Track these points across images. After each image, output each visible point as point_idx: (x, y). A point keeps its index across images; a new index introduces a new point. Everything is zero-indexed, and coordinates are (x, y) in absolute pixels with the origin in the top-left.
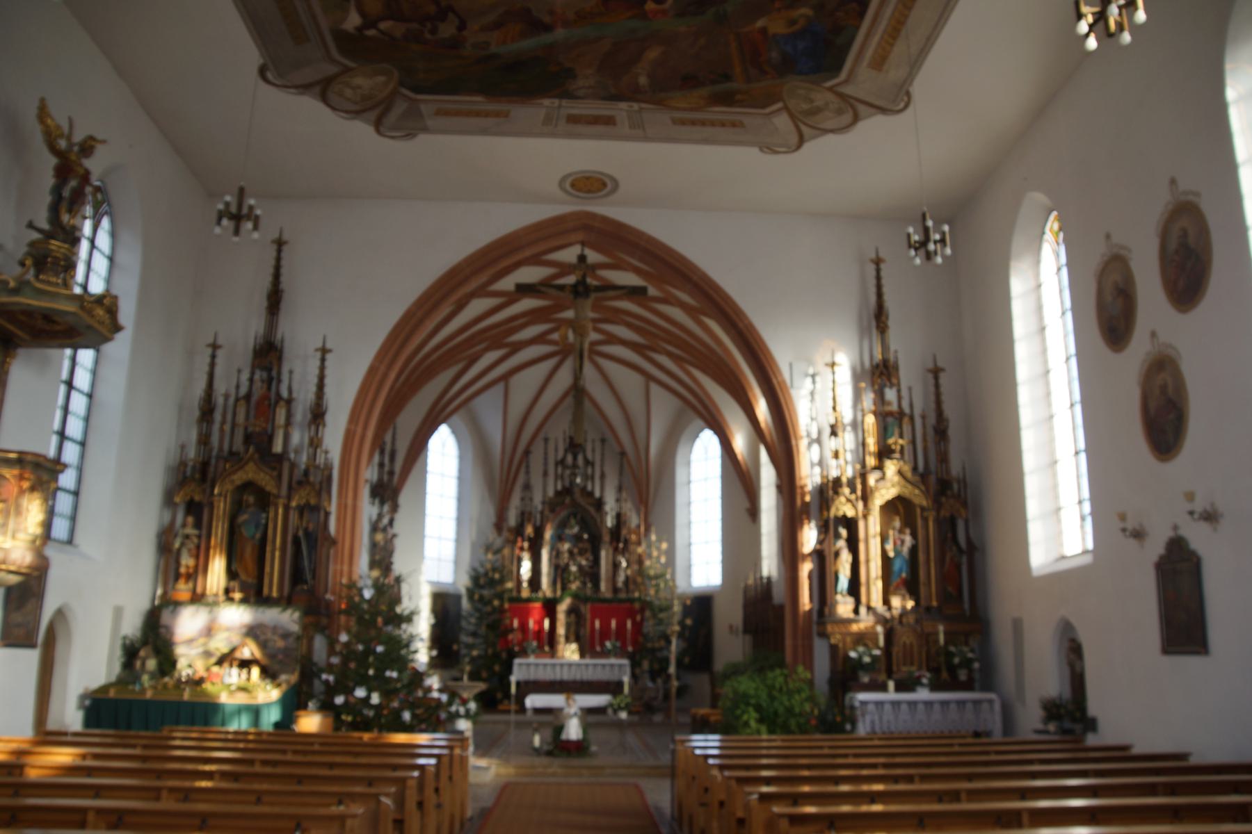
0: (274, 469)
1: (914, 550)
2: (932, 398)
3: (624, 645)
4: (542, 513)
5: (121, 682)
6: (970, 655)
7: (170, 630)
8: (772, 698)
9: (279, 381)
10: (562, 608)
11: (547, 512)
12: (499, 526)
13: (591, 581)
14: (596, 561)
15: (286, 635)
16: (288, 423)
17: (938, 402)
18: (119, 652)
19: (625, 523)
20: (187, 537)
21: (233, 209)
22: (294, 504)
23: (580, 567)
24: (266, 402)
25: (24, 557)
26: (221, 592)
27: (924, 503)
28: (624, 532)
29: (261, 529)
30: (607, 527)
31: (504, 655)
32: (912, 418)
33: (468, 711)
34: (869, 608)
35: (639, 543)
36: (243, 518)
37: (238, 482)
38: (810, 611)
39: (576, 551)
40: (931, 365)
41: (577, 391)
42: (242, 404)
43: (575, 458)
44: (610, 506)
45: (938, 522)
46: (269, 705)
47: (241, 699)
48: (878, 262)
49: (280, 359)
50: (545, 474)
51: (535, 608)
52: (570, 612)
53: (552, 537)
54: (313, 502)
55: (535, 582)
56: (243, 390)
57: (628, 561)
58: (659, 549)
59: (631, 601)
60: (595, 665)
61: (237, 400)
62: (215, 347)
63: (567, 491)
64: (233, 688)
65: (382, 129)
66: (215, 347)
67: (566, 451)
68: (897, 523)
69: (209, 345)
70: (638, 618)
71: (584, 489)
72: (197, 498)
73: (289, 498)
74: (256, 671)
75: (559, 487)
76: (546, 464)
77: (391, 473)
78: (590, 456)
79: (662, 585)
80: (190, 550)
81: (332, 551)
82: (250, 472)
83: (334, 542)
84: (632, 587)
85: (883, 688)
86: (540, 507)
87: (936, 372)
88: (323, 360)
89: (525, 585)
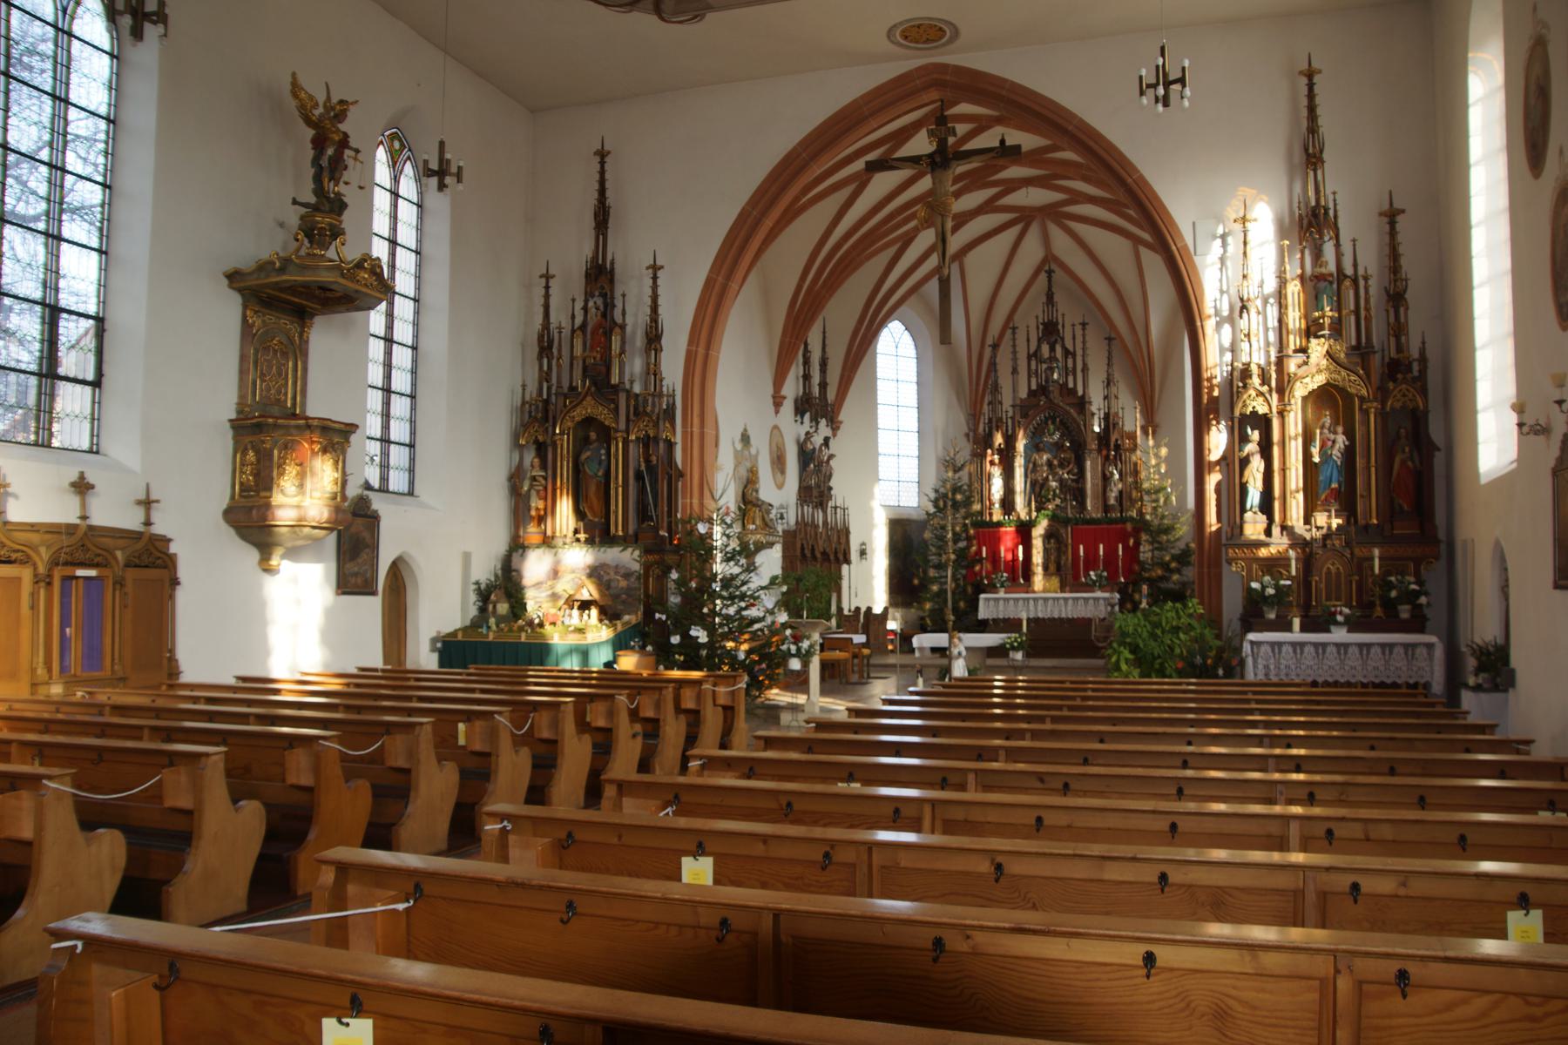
0: (613, 401)
1: (1349, 453)
2: (1387, 250)
4: (1013, 418)
5: (477, 624)
6: (1413, 587)
7: (519, 572)
8: (1153, 636)
9: (614, 306)
10: (1038, 532)
11: (1018, 418)
12: (969, 440)
15: (627, 576)
16: (623, 352)
17: (1394, 255)
18: (473, 597)
19: (1115, 425)
20: (534, 479)
21: (434, 166)
22: (633, 437)
23: (1061, 481)
24: (601, 331)
25: (322, 514)
26: (570, 534)
27: (1364, 392)
29: (605, 464)
31: (969, 589)
32: (1355, 281)
33: (799, 649)
34: (1284, 528)
36: (583, 457)
37: (578, 419)
38: (1219, 530)
39: (1056, 462)
40: (1386, 206)
41: (1049, 265)
42: (579, 332)
43: (1052, 349)
44: (1097, 404)
45: (1383, 415)
46: (599, 644)
47: (573, 640)
48: (1310, 75)
49: (612, 281)
50: (1015, 371)
51: (1006, 532)
52: (1048, 536)
53: (1026, 446)
54: (652, 434)
55: (1008, 504)
56: (579, 320)
57: (1121, 475)
58: (1157, 456)
59: (1123, 520)
60: (1074, 599)
61: (573, 331)
62: (547, 277)
63: (1043, 390)
64: (572, 628)
65: (664, 15)
66: (547, 277)
67: (1040, 341)
68: (1328, 421)
69: (541, 277)
70: (1131, 542)
71: (1063, 387)
72: (541, 438)
73: (627, 431)
74: (594, 612)
75: (1034, 387)
76: (1015, 359)
77: (823, 385)
78: (1069, 346)
79: (1162, 500)
80: (538, 492)
81: (680, 483)
82: (589, 408)
83: (681, 475)
84: (1126, 503)
85: (1288, 628)
86: (1010, 414)
87: (1391, 216)
88: (655, 278)
89: (997, 506)
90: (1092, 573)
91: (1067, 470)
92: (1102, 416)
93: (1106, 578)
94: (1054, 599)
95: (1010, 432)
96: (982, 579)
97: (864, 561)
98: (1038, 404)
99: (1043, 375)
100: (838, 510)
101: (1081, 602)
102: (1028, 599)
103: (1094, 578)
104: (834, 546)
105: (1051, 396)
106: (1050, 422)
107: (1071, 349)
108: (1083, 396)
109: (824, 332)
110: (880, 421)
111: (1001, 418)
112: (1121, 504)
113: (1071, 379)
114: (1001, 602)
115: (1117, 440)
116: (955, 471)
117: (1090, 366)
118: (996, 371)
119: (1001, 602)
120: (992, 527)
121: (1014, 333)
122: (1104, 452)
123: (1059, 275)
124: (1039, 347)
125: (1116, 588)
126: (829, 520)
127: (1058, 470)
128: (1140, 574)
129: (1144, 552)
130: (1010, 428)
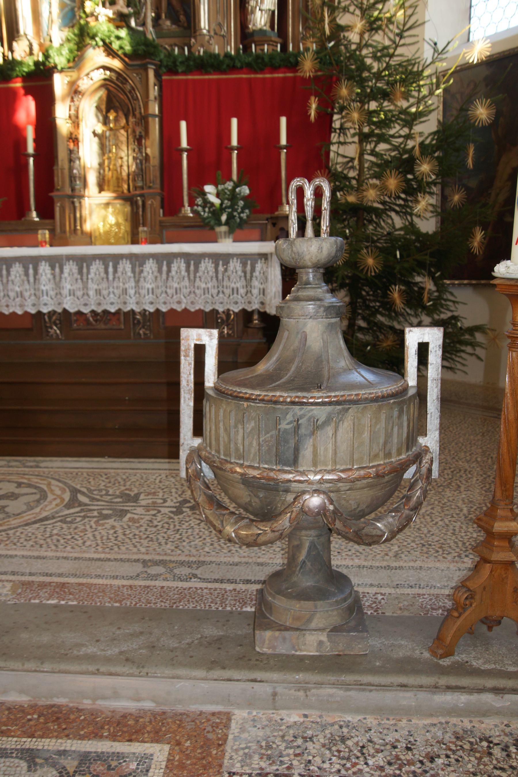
60: (158, 258)
90: (209, 189)
93: (244, 198)
94: (104, 258)
102: (36, 261)
103: (216, 201)
112: (282, 32)
129: (340, 143)
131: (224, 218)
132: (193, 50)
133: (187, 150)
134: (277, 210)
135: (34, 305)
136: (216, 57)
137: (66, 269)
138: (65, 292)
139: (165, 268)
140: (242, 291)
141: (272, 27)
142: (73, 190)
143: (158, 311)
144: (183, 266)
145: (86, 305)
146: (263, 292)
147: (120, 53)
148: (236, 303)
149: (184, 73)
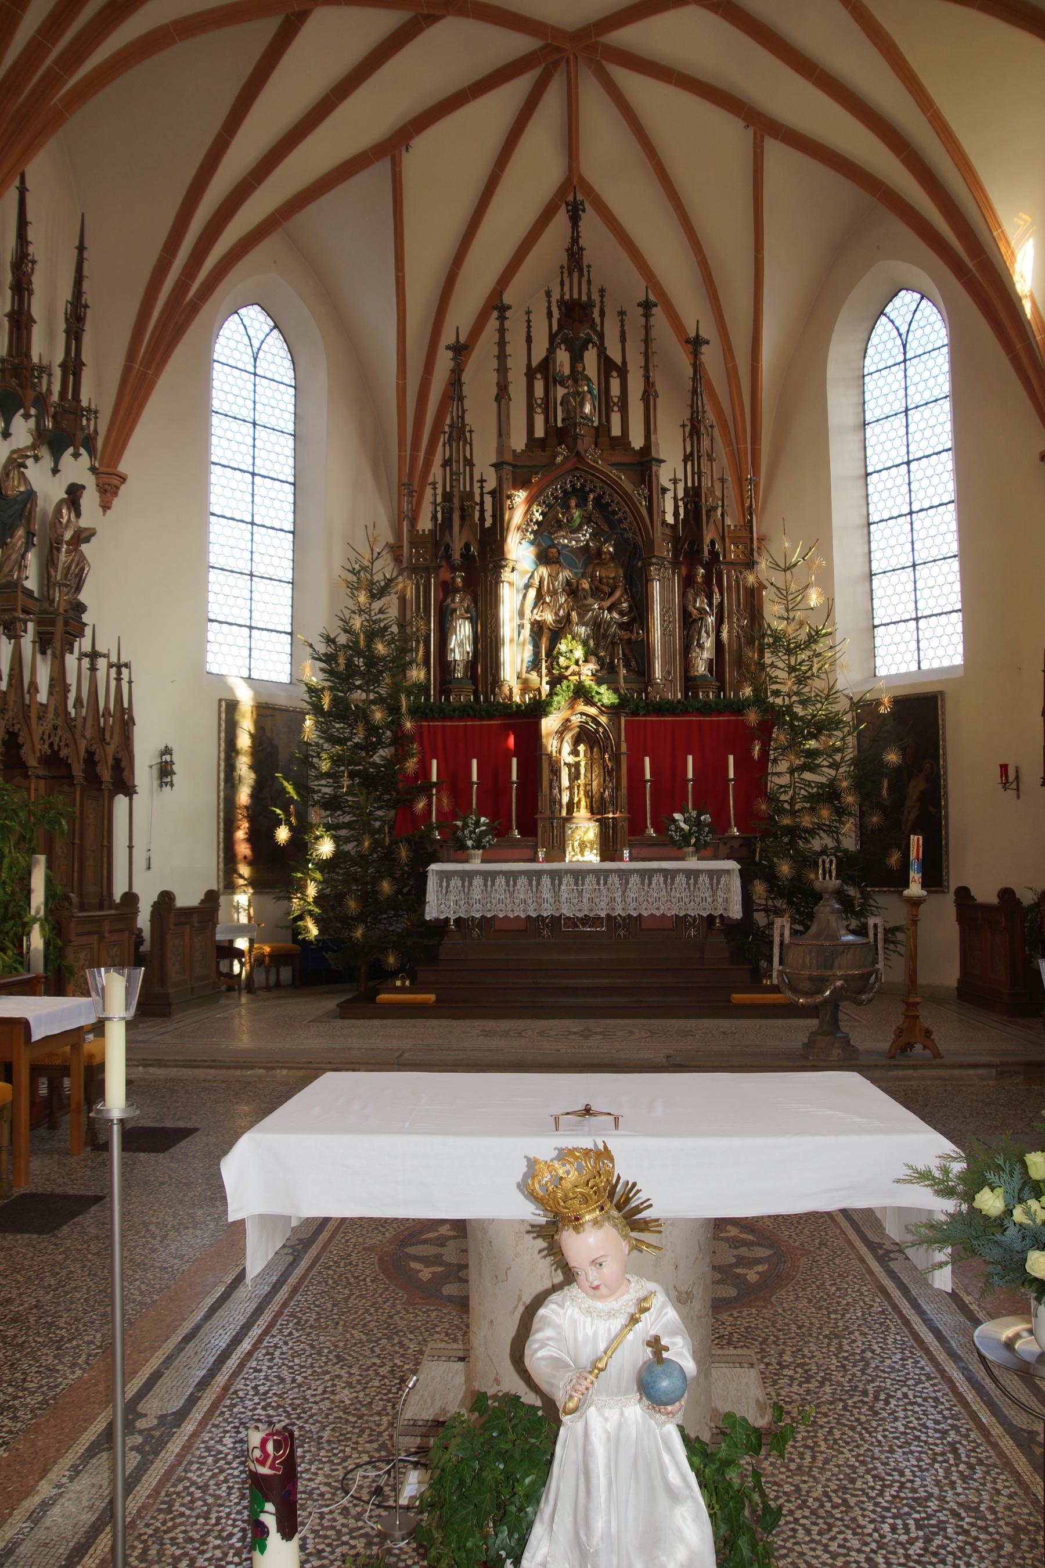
3: (720, 825)
12: (395, 550)
13: (627, 665)
14: (639, 613)
23: (598, 627)
28: (709, 535)
30: (664, 522)
31: (403, 853)
35: (750, 564)
39: (585, 585)
43: (577, 358)
59: (738, 707)
60: (642, 873)
67: (552, 337)
75: (539, 432)
76: (502, 370)
77: (73, 367)
78: (614, 353)
84: (730, 673)
86: (491, 485)
90: (677, 816)
91: (607, 604)
92: (681, 494)
93: (707, 825)
95: (488, 524)
96: (430, 829)
97: (167, 789)
98: (553, 462)
99: (559, 409)
100: (102, 663)
101: (658, 880)
102: (539, 874)
103: (686, 827)
104: (83, 744)
105: (580, 446)
106: (573, 503)
107: (618, 361)
108: (647, 448)
109: (81, 248)
110: (213, 498)
111: (471, 493)
112: (720, 677)
113: (616, 418)
114: (478, 881)
115: (713, 543)
116: (373, 597)
117: (659, 387)
118: (461, 399)
119: (478, 881)
120: (451, 719)
121: (502, 318)
122: (684, 571)
123: (589, 219)
124: (551, 351)
125: (724, 849)
126: (71, 679)
127: (590, 601)
128: (772, 818)
130: (488, 515)
131: (693, 841)
132: (650, 696)
133: (649, 781)
134: (727, 831)
135: (535, 910)
136: (668, 701)
137: (565, 881)
138: (563, 899)
139: (646, 881)
140: (709, 900)
141: (710, 671)
142: (552, 812)
143: (629, 915)
144: (662, 880)
145: (580, 910)
146: (726, 900)
147: (599, 704)
148: (705, 909)
149: (644, 715)
